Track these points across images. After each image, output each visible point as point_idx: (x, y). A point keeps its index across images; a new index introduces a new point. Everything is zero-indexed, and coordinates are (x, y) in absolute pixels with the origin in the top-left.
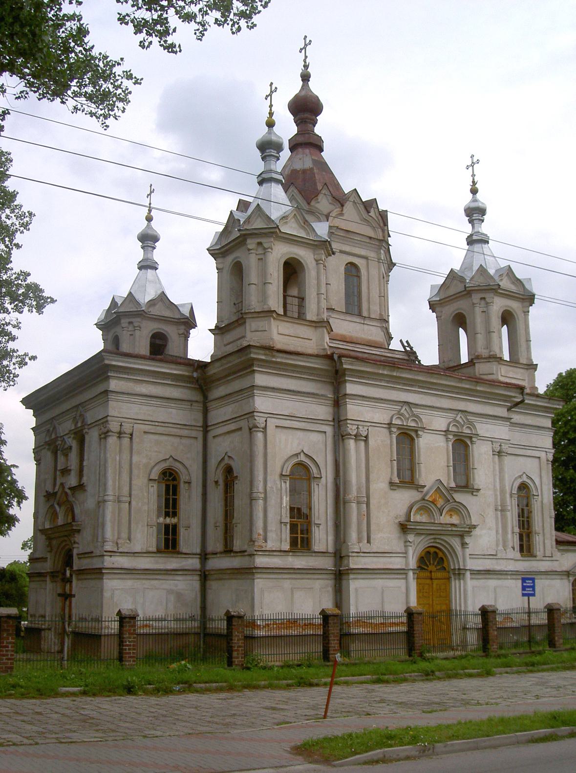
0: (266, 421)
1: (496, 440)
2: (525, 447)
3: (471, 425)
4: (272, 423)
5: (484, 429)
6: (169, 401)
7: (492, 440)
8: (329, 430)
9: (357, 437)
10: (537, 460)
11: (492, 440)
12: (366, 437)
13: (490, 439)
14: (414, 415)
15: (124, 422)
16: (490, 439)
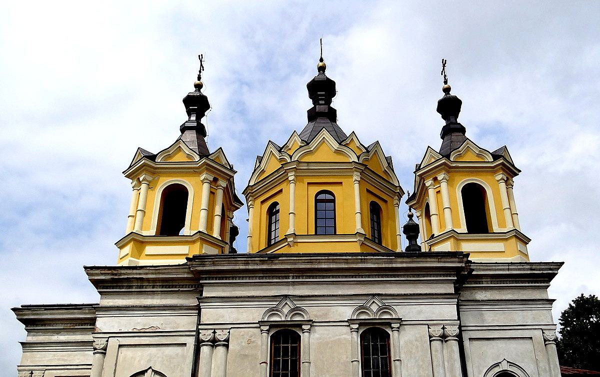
0: (107, 341)
1: (435, 322)
2: (502, 328)
3: (385, 309)
4: (114, 343)
5: (404, 311)
6: (86, 344)
7: (428, 322)
8: (191, 341)
9: (214, 343)
10: (530, 341)
11: (428, 322)
12: (227, 340)
13: (425, 322)
14: (297, 309)
15: (36, 370)
16: (425, 322)
